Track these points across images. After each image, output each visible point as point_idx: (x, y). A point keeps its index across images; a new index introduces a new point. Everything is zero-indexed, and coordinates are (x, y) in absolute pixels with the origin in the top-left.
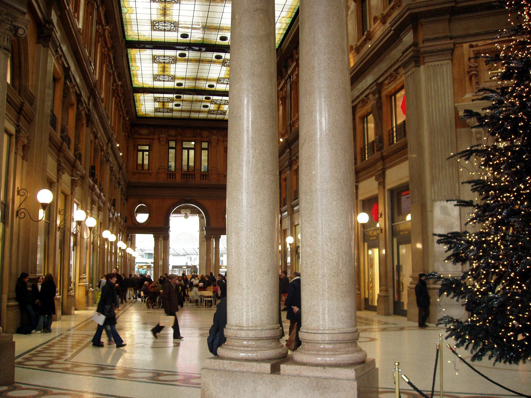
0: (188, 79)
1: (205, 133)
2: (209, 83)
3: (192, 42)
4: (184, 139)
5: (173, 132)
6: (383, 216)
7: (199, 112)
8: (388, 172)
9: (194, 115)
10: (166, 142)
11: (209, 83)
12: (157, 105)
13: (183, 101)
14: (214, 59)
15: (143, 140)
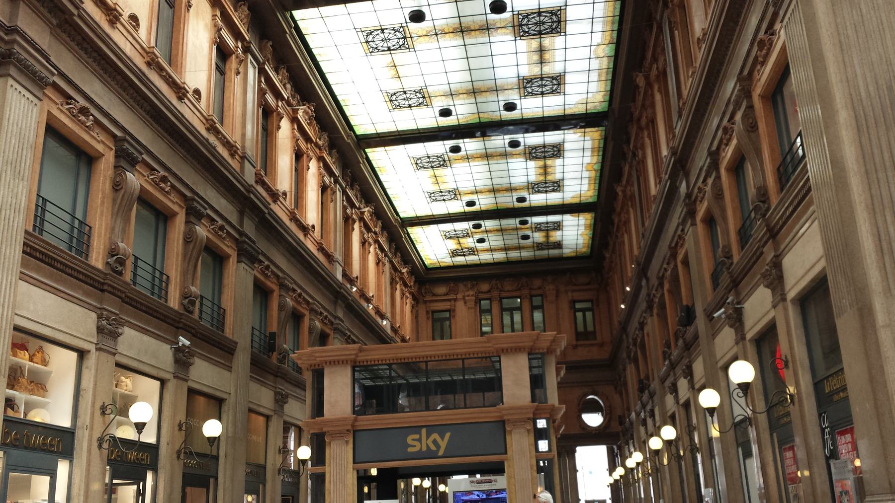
0: (481, 192)
1: (537, 283)
2: (516, 195)
3: (462, 122)
4: (504, 294)
5: (485, 287)
6: (790, 365)
7: (519, 248)
8: (788, 262)
9: (514, 255)
10: (476, 303)
11: (516, 195)
12: (452, 245)
13: (487, 231)
14: (509, 149)
15: (435, 304)
